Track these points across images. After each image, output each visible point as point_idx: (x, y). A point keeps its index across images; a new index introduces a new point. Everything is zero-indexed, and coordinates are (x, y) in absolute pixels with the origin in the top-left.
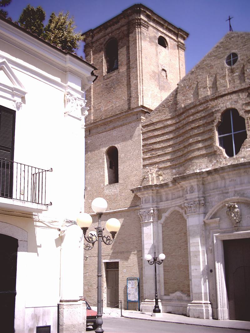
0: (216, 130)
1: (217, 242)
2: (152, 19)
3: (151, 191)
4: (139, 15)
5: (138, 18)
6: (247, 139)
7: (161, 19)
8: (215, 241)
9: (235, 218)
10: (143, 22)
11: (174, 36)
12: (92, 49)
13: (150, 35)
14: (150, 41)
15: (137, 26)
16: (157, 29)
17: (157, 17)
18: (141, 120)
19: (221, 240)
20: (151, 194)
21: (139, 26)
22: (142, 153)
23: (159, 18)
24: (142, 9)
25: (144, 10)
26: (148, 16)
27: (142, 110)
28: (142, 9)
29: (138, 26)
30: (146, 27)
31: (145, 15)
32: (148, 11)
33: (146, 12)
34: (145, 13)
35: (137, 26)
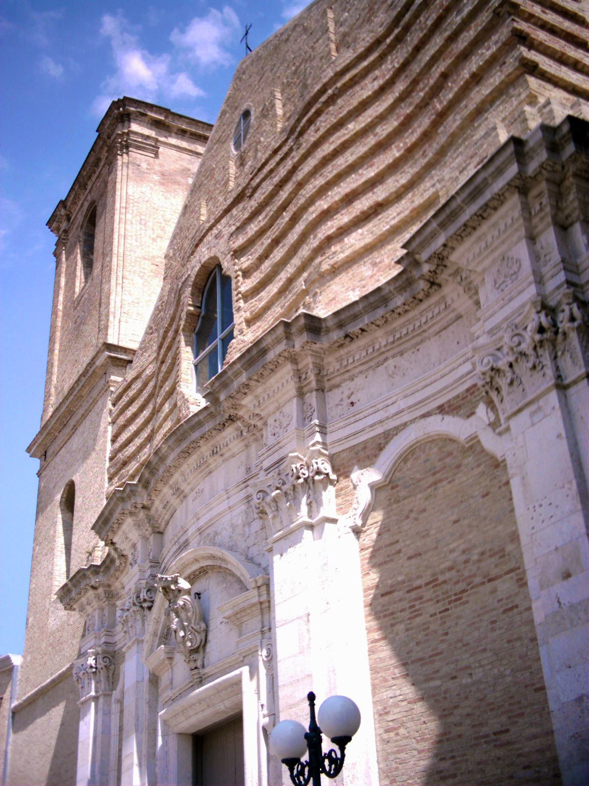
0: (183, 343)
1: (165, 743)
2: (175, 130)
3: (91, 593)
4: (126, 124)
5: (123, 133)
6: (234, 341)
7: (206, 126)
8: (160, 742)
9: (182, 634)
10: (140, 140)
11: (177, 138)
12: (64, 246)
13: (165, 168)
14: (163, 181)
15: (119, 152)
16: (191, 151)
17: (187, 124)
18: (109, 387)
19: (180, 734)
20: (95, 604)
21: (124, 151)
22: (107, 480)
23: (197, 125)
24: (132, 109)
25: (138, 110)
26: (157, 124)
27: (110, 357)
28: (132, 109)
29: (121, 150)
30: (144, 148)
31: (148, 123)
32: (152, 111)
33: (145, 115)
34: (146, 119)
35: (119, 152)
